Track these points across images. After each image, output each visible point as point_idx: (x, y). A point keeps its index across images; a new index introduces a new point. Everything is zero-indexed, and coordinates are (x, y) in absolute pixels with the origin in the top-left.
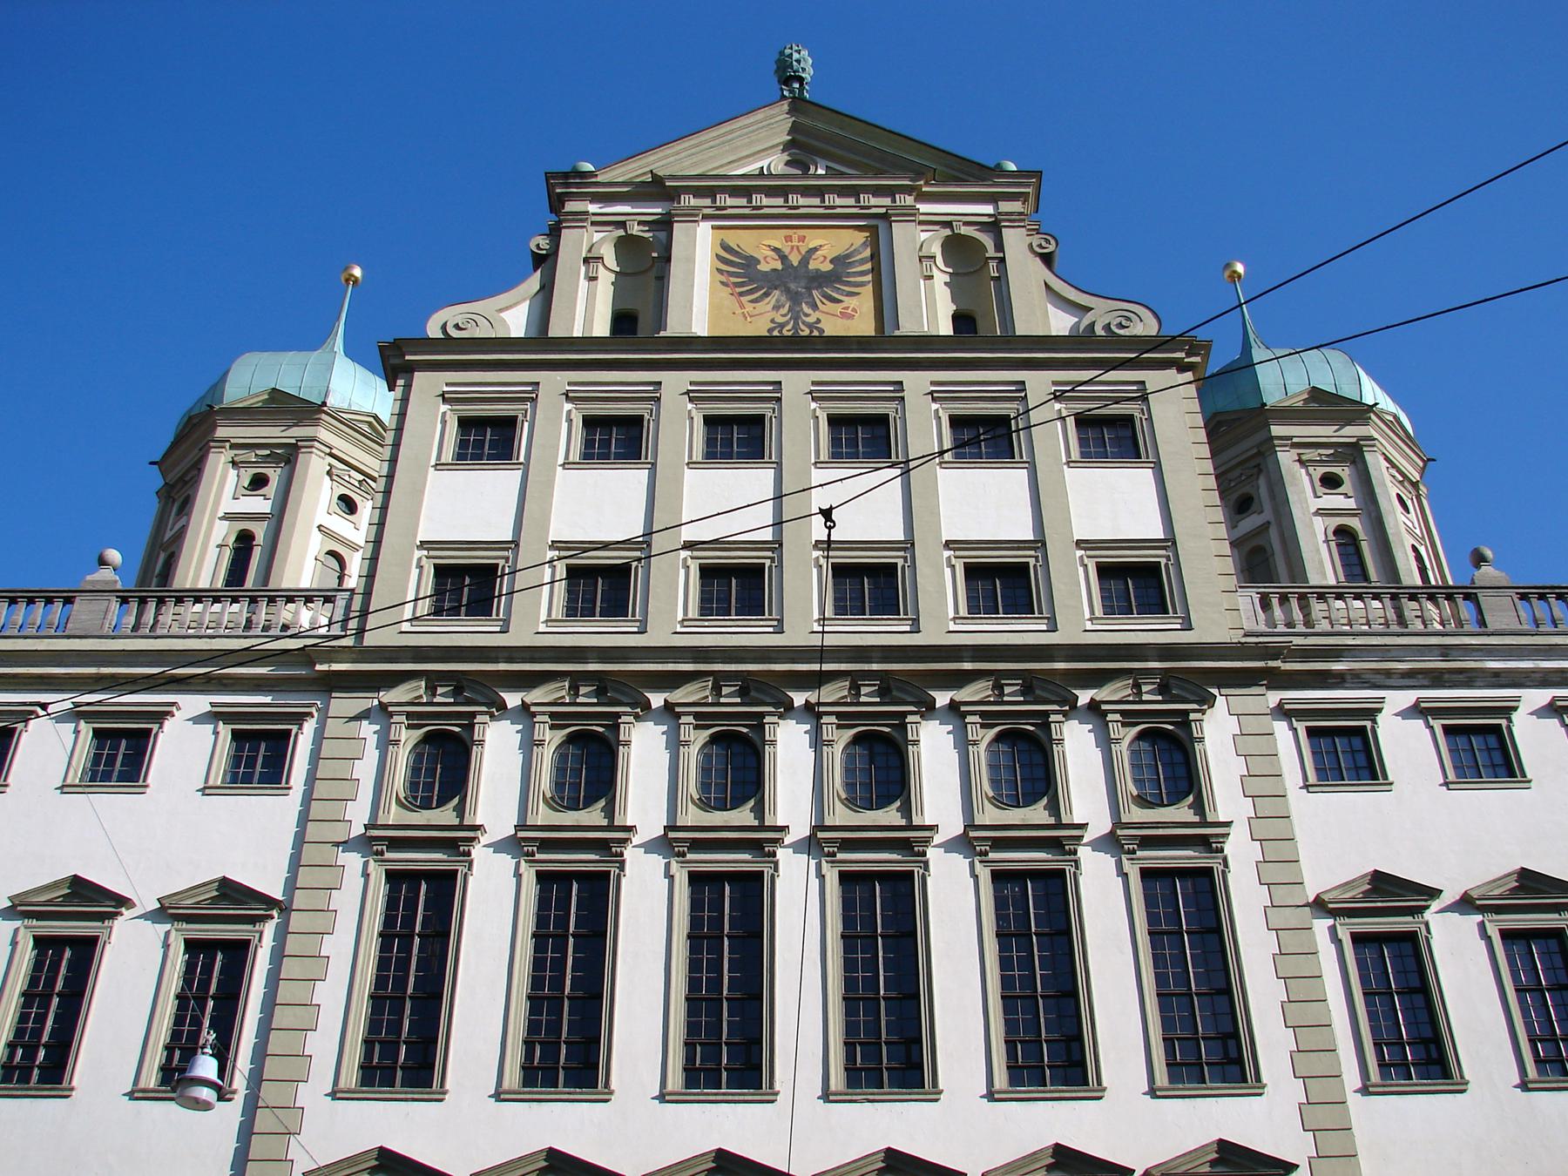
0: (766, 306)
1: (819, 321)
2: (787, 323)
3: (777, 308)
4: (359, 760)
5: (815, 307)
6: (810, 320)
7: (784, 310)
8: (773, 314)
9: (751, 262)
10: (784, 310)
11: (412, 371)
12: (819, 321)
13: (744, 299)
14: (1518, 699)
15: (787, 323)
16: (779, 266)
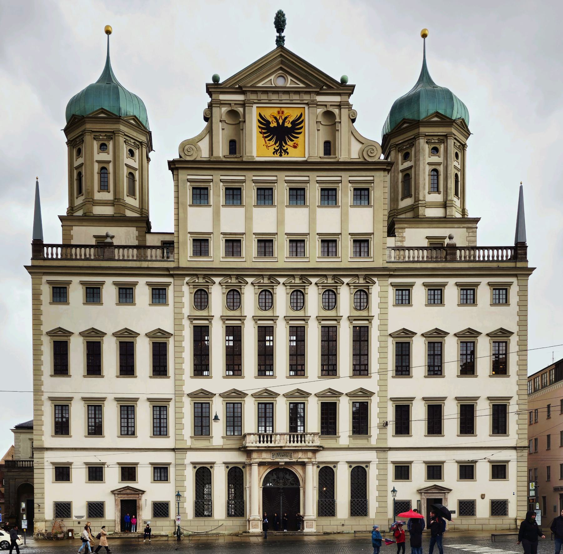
0: (272, 142)
1: (287, 149)
2: (278, 150)
3: (275, 144)
4: (182, 294)
5: (286, 144)
6: (285, 148)
7: (277, 145)
8: (274, 146)
9: (268, 123)
10: (277, 145)
11: (178, 170)
12: (287, 149)
13: (267, 139)
14: (448, 283)
15: (278, 150)
16: (276, 125)
